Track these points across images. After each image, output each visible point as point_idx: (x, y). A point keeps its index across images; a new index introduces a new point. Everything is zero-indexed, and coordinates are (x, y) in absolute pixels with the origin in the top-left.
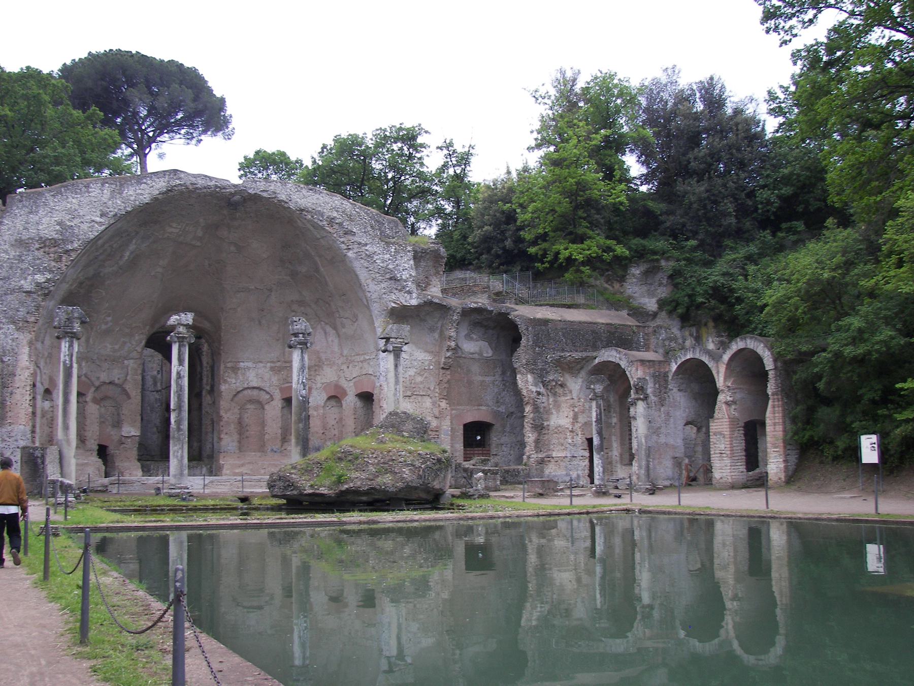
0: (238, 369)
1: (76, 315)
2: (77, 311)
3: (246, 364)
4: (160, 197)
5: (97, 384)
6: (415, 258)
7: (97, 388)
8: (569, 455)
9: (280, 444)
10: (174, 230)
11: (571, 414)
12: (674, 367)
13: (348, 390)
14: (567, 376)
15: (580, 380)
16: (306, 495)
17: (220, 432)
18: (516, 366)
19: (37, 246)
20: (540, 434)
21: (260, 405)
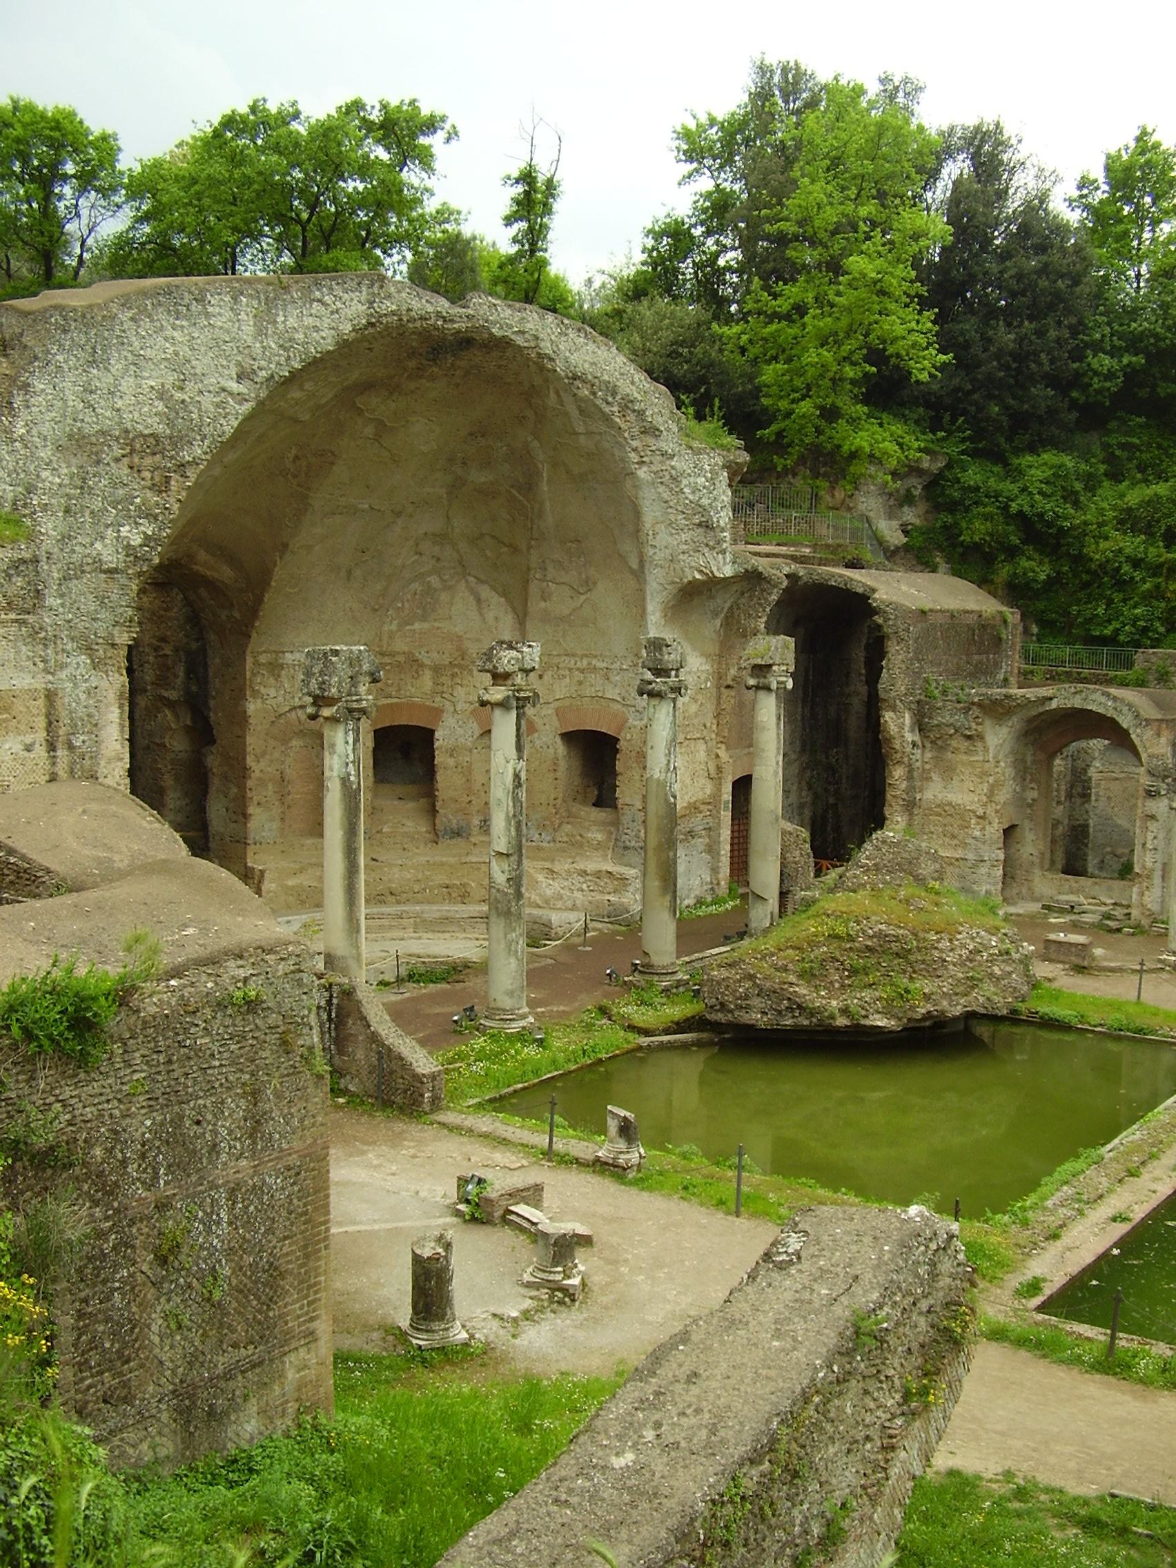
0: (282, 667)
8: (971, 856)
19: (118, 452)
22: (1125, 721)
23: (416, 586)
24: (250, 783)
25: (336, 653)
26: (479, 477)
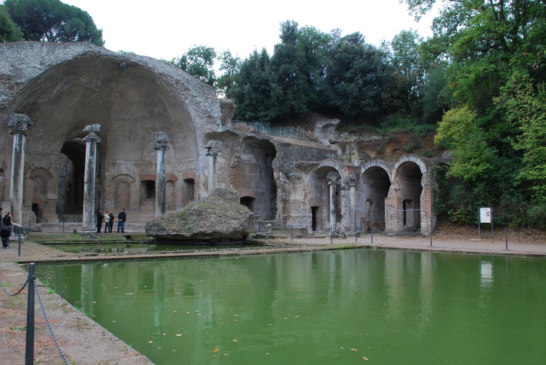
1: (25, 120)
2: (26, 118)
3: (120, 161)
4: (79, 57)
5: (33, 168)
6: (221, 107)
7: (33, 170)
8: (301, 215)
9: (138, 206)
10: (84, 80)
11: (304, 193)
12: (363, 170)
13: (179, 179)
14: (302, 173)
15: (309, 176)
16: (172, 235)
17: (104, 198)
18: (273, 167)
20: (285, 204)
21: (128, 184)
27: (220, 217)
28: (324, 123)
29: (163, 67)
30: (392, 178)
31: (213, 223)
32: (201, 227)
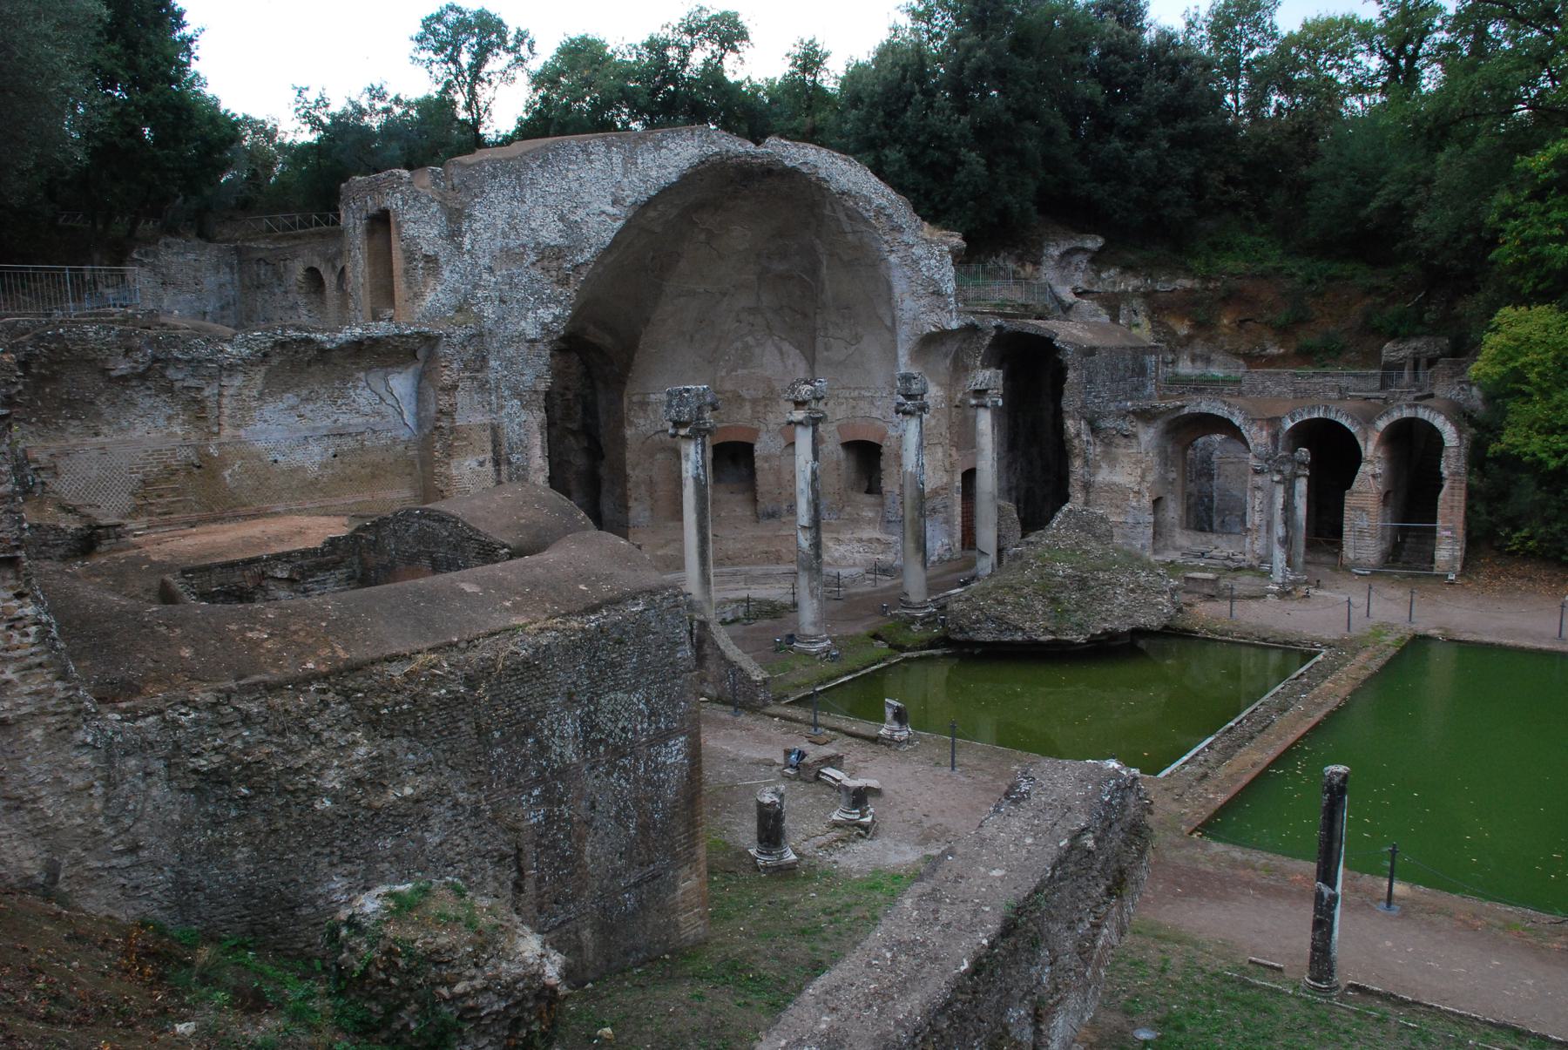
0: (648, 404)
8: (1130, 520)
12: (1289, 425)
14: (1140, 425)
19: (533, 258)
22: (1237, 421)
23: (739, 344)
24: (629, 485)
25: (688, 391)
26: (779, 267)
27: (1132, 591)
28: (1065, 246)
29: (844, 173)
30: (1370, 447)
31: (1126, 609)
32: (1105, 620)
